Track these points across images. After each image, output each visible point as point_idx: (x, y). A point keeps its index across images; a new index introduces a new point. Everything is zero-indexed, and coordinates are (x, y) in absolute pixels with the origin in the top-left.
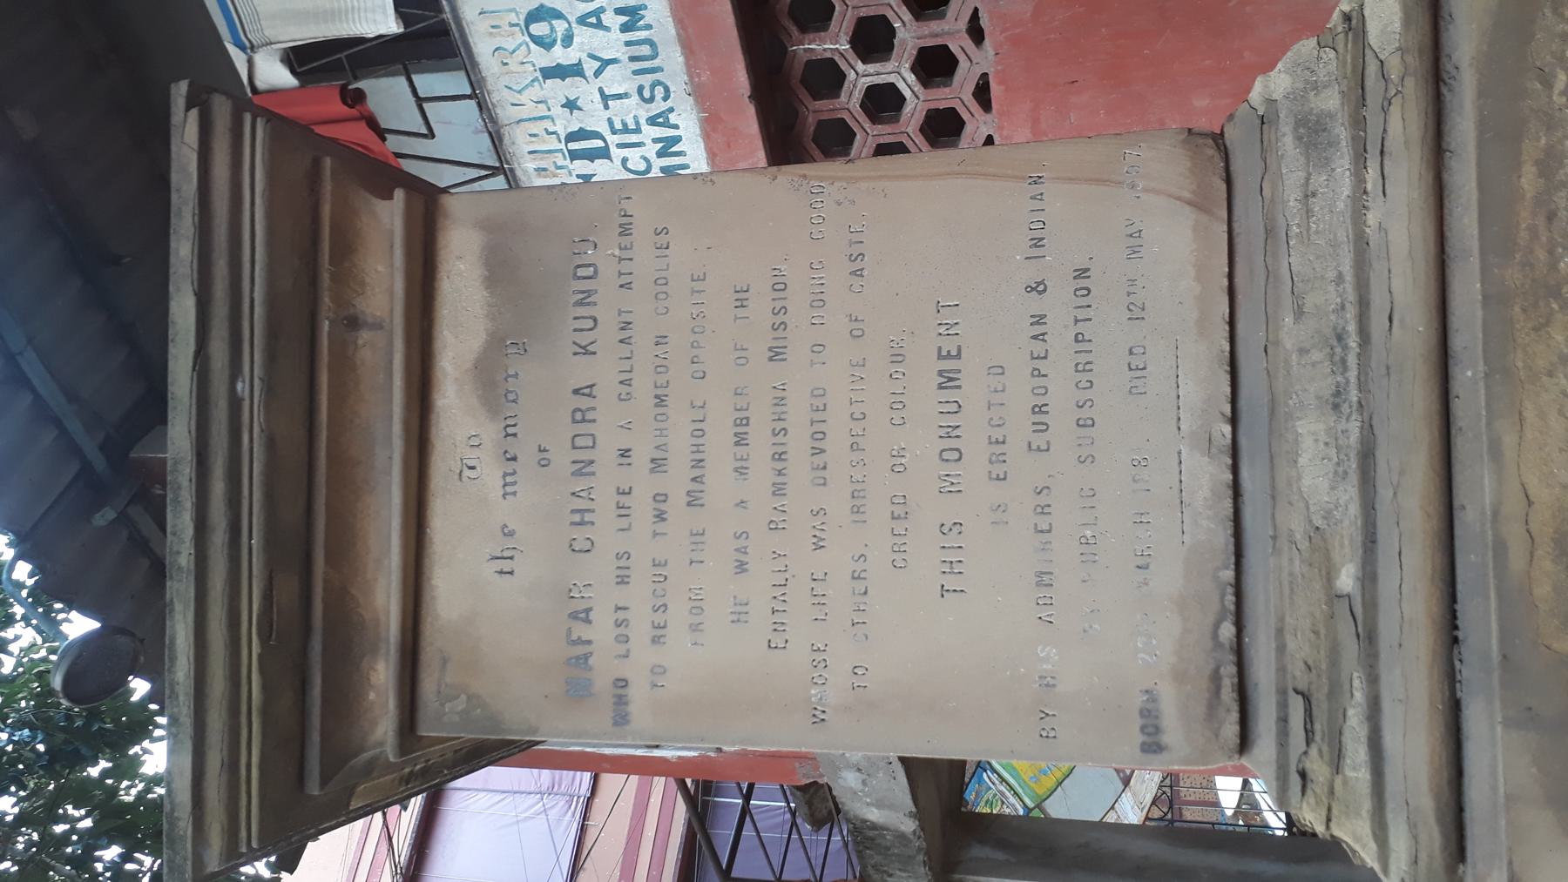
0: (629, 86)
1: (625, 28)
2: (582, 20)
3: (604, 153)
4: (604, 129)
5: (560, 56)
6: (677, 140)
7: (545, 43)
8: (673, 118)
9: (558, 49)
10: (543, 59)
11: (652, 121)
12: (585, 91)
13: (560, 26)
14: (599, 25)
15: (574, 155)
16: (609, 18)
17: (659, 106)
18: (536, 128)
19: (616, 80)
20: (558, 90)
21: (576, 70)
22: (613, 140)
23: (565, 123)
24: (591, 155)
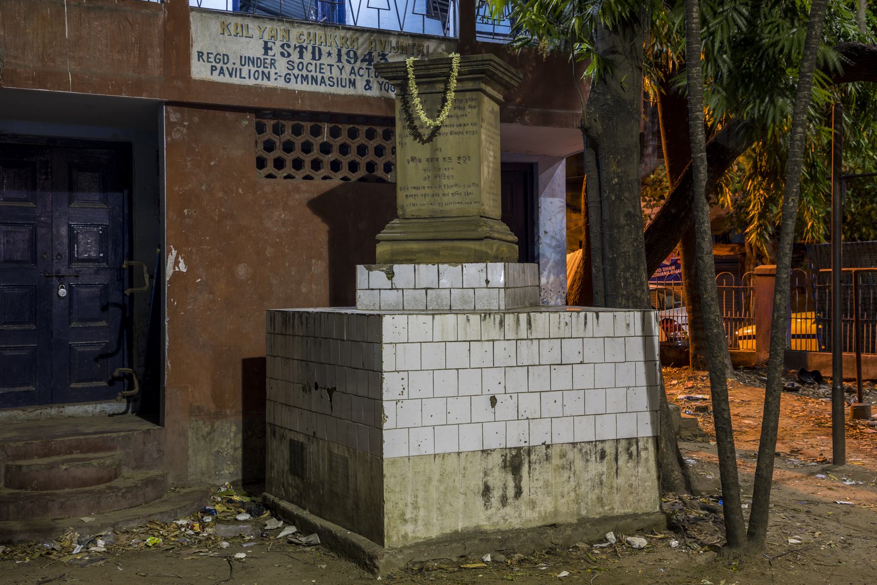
0: (333, 75)
1: (350, 80)
2: (353, 68)
3: (314, 58)
4: (321, 61)
5: (344, 57)
6: (317, 84)
7: (348, 54)
8: (323, 85)
9: (346, 57)
10: (344, 51)
11: (323, 78)
12: (333, 60)
13: (352, 61)
14: (351, 73)
15: (314, 48)
16: (353, 76)
17: (327, 82)
18: (323, 39)
19: (336, 72)
20: (334, 52)
21: (339, 61)
22: (318, 63)
23: (325, 49)
24: (313, 53)
